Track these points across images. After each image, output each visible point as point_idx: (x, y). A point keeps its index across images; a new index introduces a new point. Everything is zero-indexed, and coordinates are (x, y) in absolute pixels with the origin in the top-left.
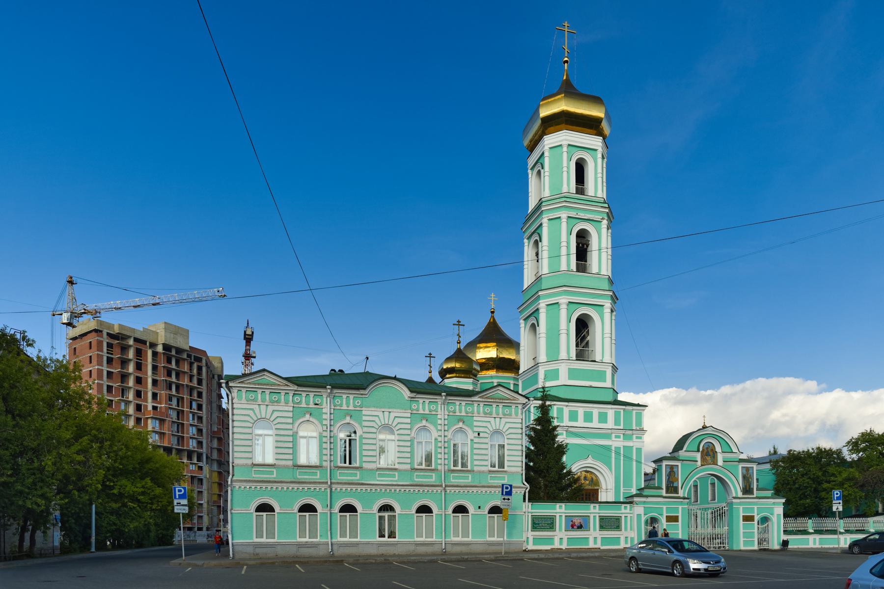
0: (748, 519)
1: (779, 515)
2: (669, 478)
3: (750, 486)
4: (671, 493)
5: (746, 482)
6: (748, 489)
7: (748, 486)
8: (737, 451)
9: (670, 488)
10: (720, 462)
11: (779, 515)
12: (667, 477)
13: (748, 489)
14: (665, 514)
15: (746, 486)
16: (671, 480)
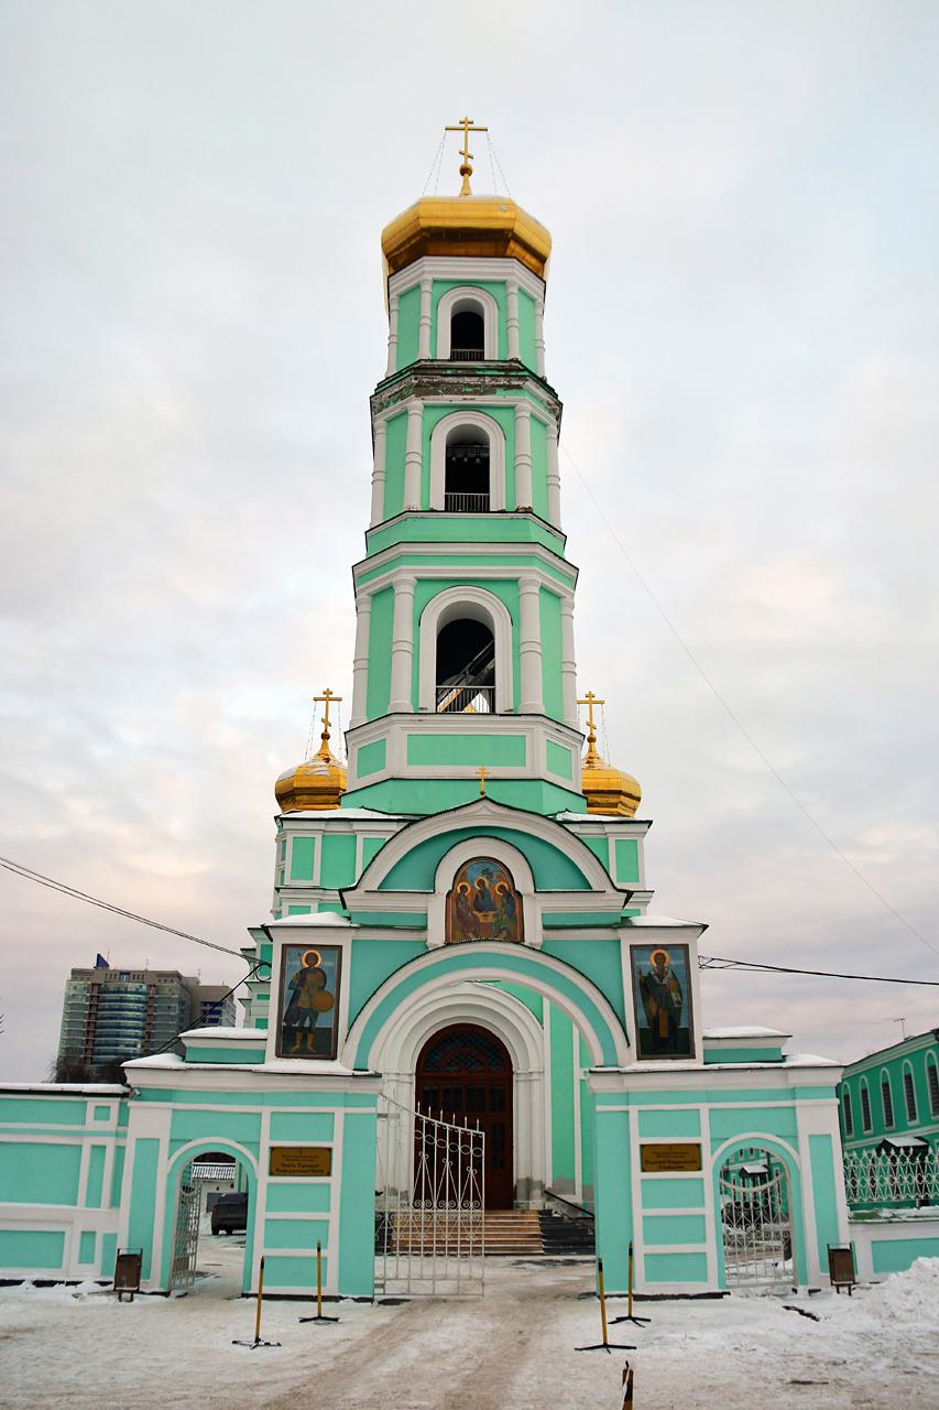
0: (662, 1158)
1: (820, 1139)
2: (294, 999)
3: (673, 1022)
4: (304, 1054)
5: (654, 1008)
6: (664, 1033)
7: (663, 1023)
8: (610, 890)
9: (299, 1036)
10: (533, 932)
11: (820, 1139)
12: (288, 993)
13: (664, 1033)
14: (266, 1143)
15: (654, 1021)
16: (303, 1002)
